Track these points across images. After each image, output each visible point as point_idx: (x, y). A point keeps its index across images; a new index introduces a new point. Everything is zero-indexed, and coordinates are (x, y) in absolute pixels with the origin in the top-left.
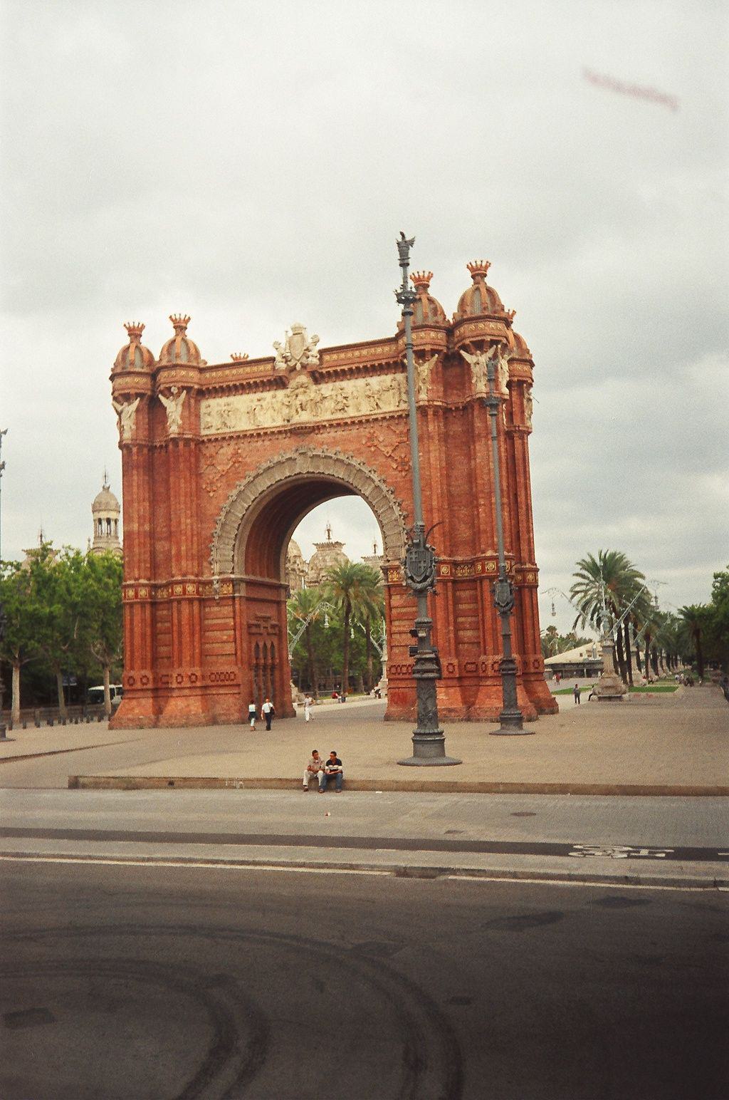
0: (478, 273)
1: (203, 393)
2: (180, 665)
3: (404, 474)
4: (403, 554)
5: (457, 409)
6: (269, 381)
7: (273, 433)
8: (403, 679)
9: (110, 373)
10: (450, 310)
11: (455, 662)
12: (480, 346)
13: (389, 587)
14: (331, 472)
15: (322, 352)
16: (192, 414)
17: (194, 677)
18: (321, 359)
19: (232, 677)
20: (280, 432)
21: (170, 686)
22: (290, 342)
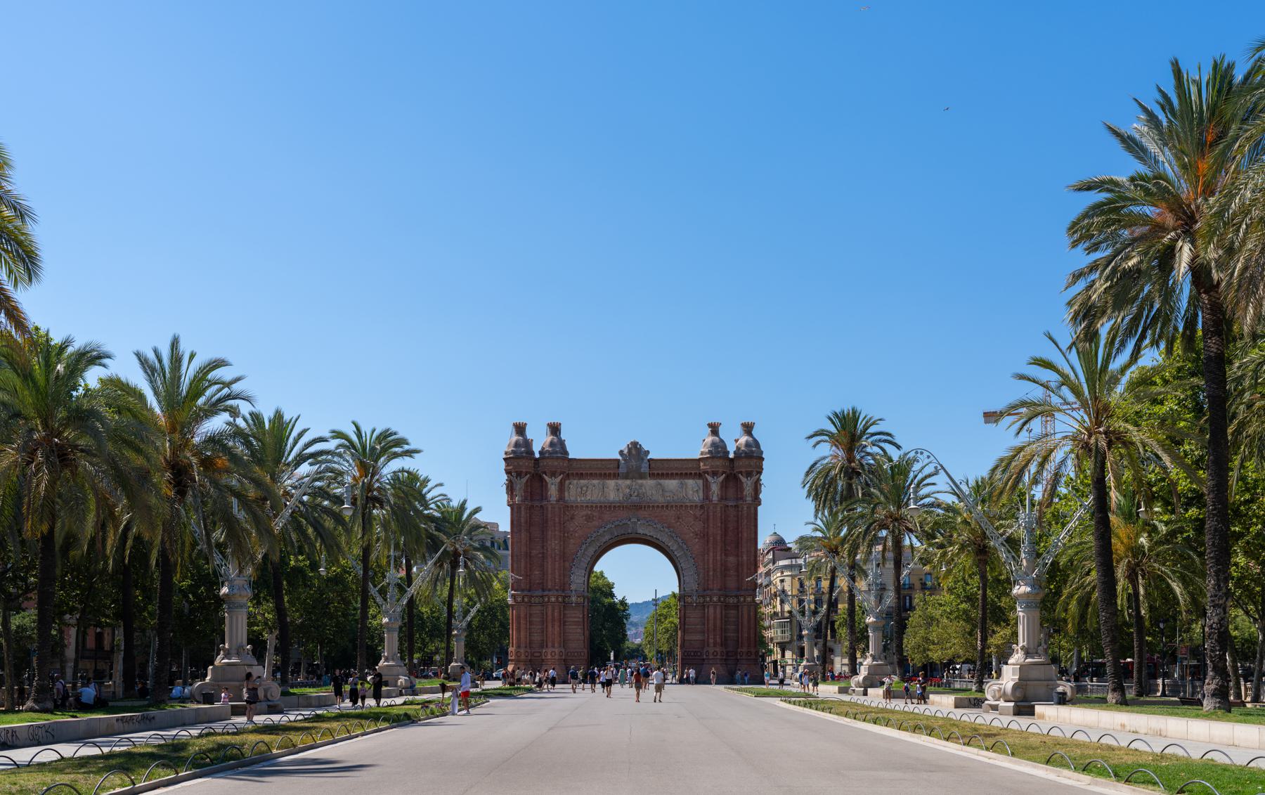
4: (695, 587)
12: (749, 474)
22: (630, 450)
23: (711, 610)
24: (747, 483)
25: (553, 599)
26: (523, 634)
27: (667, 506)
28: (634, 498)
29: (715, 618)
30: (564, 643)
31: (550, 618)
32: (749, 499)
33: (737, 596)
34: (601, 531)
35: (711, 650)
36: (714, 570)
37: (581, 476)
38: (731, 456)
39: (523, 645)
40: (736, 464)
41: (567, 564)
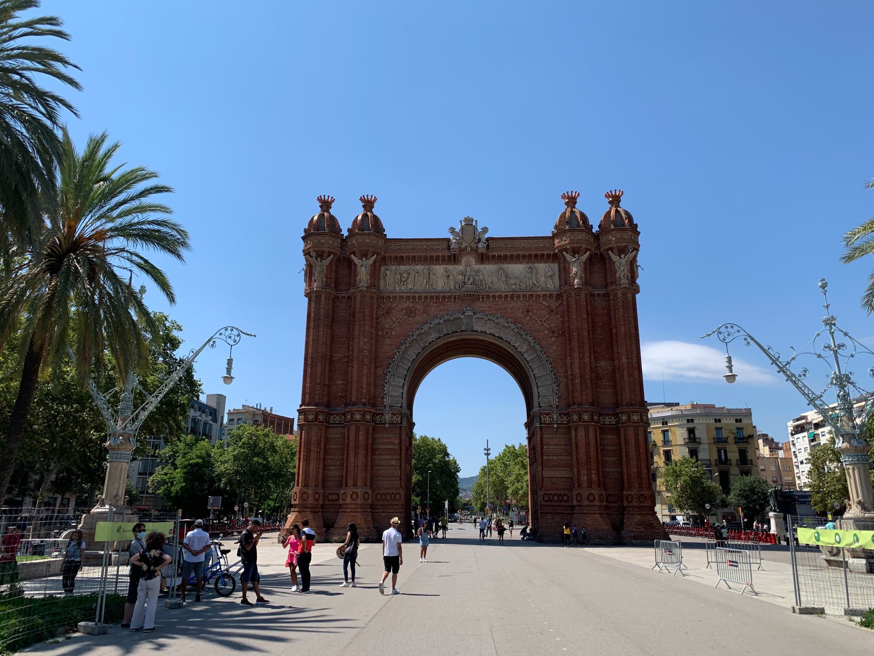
0: (615, 200)
1: (383, 260)
2: (355, 485)
3: (554, 339)
4: (554, 401)
5: (598, 294)
6: (443, 257)
7: (444, 297)
8: (553, 506)
9: (303, 234)
10: (595, 222)
11: (604, 493)
12: (622, 251)
13: (541, 428)
14: (492, 331)
15: (488, 239)
16: (375, 273)
17: (366, 496)
18: (488, 246)
19: (398, 497)
20: (450, 297)
21: (341, 502)
22: (462, 228)
23: (581, 433)
24: (620, 263)
25: (358, 417)
26: (312, 467)
27: (512, 297)
28: (469, 286)
29: (588, 444)
30: (372, 481)
31: (352, 444)
32: (624, 281)
33: (616, 415)
34: (426, 327)
35: (585, 493)
36: (582, 377)
37: (400, 260)
38: (595, 229)
39: (312, 483)
40: (603, 239)
41: (380, 372)
